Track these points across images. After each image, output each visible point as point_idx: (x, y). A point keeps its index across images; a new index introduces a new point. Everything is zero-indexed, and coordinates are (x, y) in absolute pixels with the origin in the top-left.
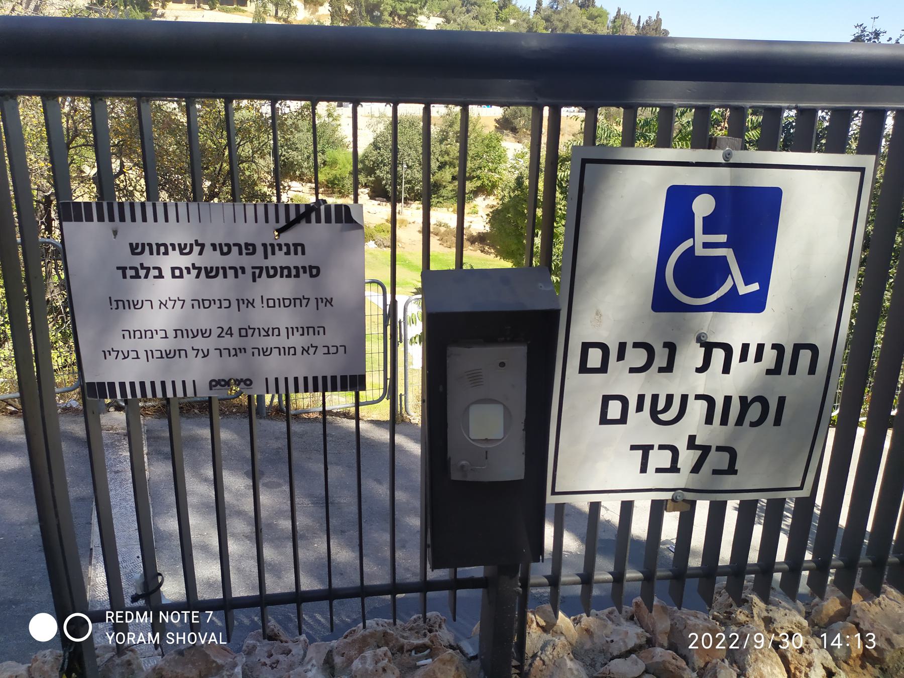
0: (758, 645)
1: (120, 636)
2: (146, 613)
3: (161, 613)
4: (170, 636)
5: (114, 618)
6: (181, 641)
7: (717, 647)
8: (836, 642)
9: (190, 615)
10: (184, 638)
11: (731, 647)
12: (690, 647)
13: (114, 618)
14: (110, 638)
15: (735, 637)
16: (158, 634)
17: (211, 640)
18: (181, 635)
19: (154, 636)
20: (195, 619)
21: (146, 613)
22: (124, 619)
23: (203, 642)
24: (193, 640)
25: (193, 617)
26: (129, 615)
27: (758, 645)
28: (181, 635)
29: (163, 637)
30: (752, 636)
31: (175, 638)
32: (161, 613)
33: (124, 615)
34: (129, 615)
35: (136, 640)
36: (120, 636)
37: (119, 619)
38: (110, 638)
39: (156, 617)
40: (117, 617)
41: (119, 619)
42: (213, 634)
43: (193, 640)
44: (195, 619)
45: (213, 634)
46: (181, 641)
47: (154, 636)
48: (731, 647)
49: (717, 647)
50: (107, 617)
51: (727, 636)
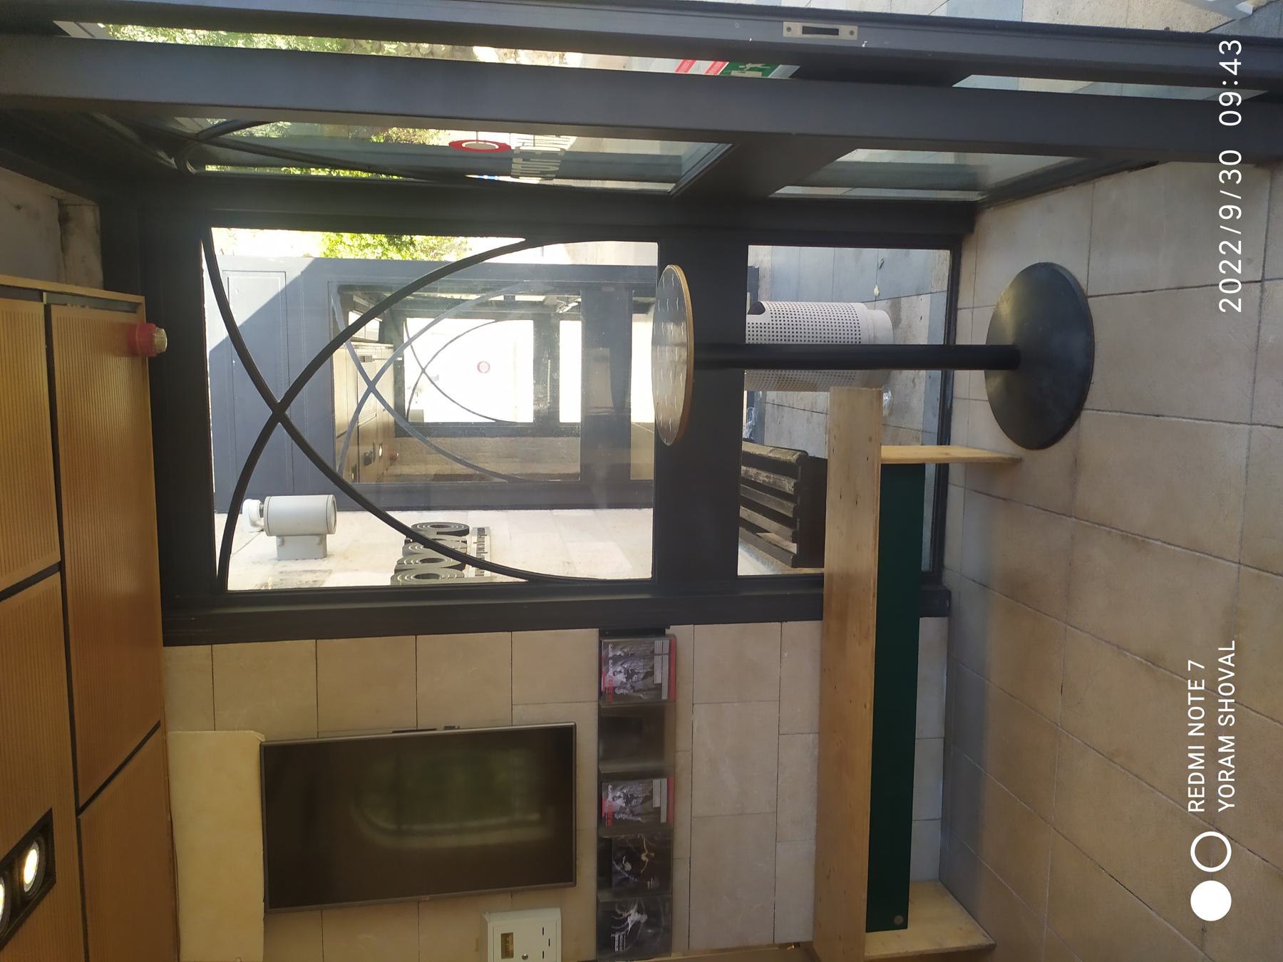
0: (1236, 212)
1: (1224, 791)
2: (1191, 755)
3: (1191, 733)
4: (1223, 721)
5: (1198, 800)
6: (1230, 706)
7: (1239, 271)
8: (1232, 67)
9: (1194, 693)
10: (1226, 701)
11: (1239, 252)
12: (1239, 309)
13: (1198, 800)
14: (1227, 805)
15: (1225, 247)
16: (1221, 738)
17: (1229, 663)
18: (1223, 705)
19: (1226, 744)
20: (1200, 685)
21: (1191, 755)
22: (1199, 787)
23: (1232, 674)
24: (1229, 689)
25: (1196, 688)
26: (1194, 778)
27: (1236, 212)
28: (1223, 705)
29: (1227, 730)
30: (1226, 223)
31: (1226, 714)
32: (1191, 733)
33: (1193, 786)
34: (1194, 778)
35: (1229, 769)
36: (1224, 791)
37: (1200, 793)
38: (1227, 805)
39: (1195, 741)
40: (1196, 796)
41: (1200, 793)
42: (1221, 660)
43: (1229, 689)
44: (1200, 685)
45: (1221, 660)
46: (1230, 706)
47: (1226, 744)
48: (1239, 252)
49: (1239, 271)
50: (1197, 810)
51: (1223, 257)
